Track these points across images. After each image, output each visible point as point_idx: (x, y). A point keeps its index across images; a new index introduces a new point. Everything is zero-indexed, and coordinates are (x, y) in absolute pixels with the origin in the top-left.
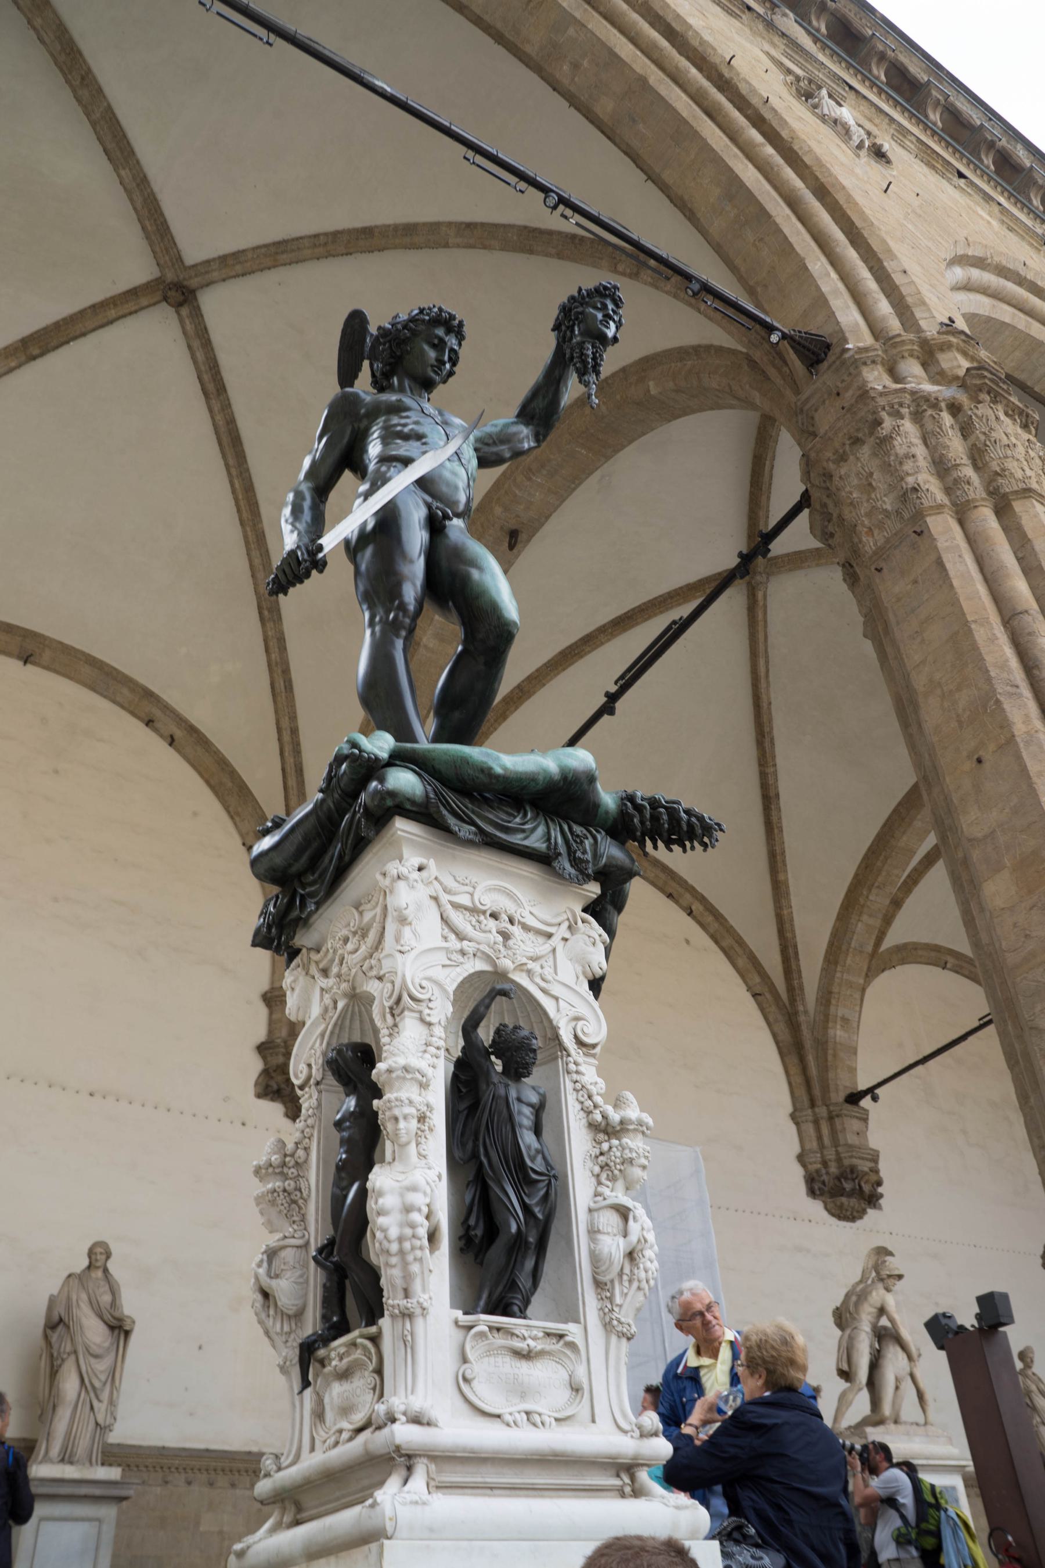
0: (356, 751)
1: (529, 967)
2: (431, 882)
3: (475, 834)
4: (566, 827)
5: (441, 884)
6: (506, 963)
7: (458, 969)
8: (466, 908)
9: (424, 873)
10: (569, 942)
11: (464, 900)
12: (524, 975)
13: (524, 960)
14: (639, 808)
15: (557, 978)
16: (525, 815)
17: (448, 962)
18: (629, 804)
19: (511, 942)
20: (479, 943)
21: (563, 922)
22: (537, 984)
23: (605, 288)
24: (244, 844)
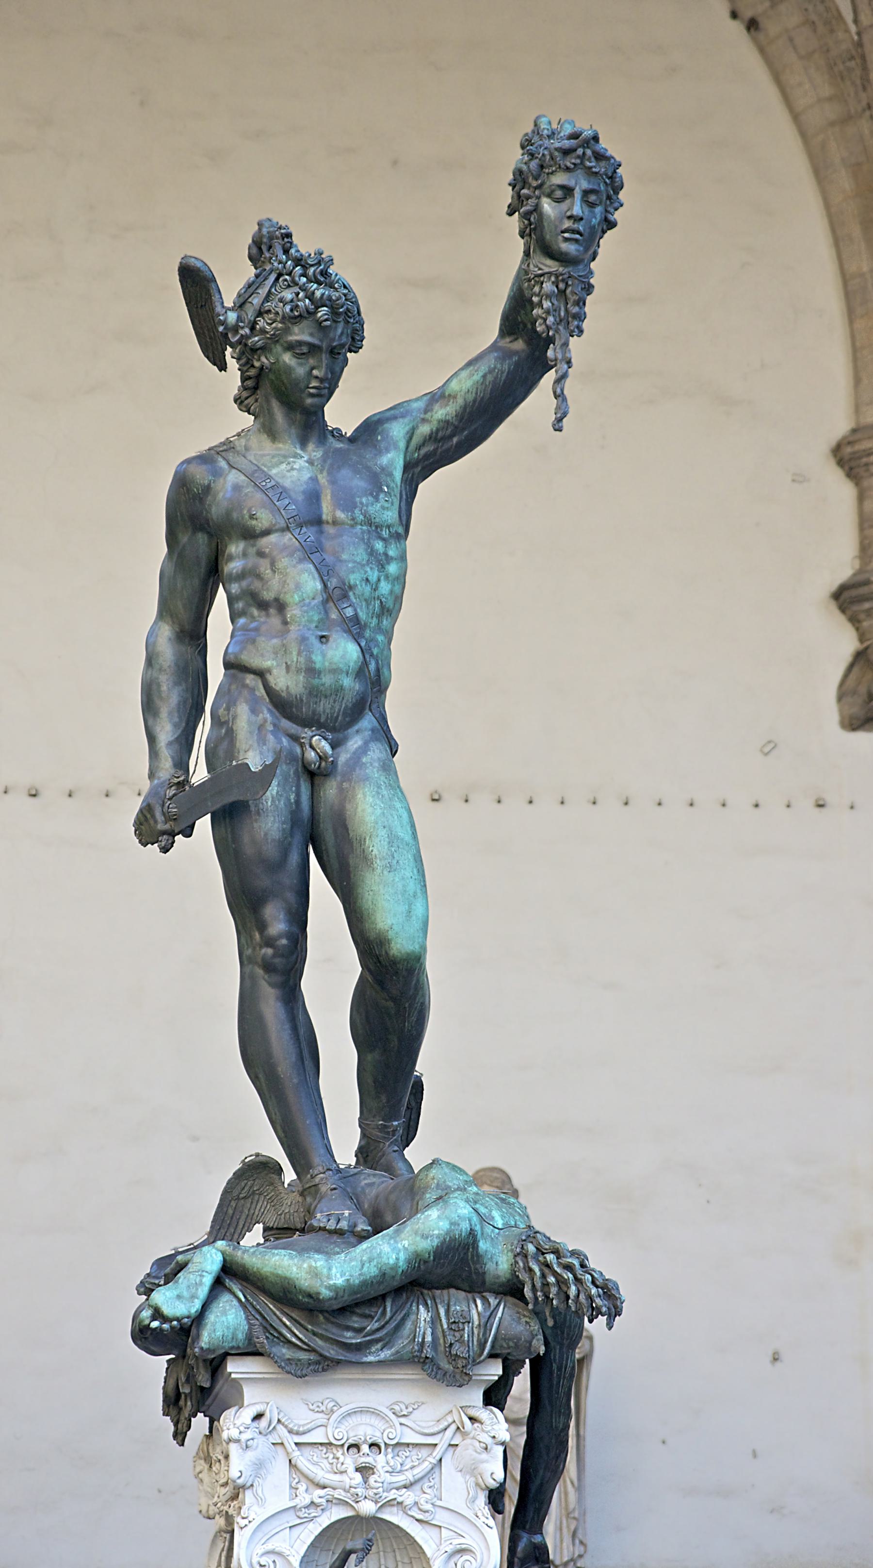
0: (155, 1324)
1: (400, 1499)
2: (274, 1428)
3: (318, 1363)
4: (442, 1312)
5: (286, 1427)
6: (367, 1508)
7: (311, 1525)
8: (321, 1444)
9: (264, 1423)
10: (459, 1448)
11: (317, 1436)
12: (395, 1509)
13: (393, 1494)
14: (531, 1270)
15: (438, 1503)
16: (384, 1313)
17: (299, 1521)
18: (521, 1264)
19: (372, 1479)
20: (334, 1489)
21: (449, 1426)
22: (412, 1516)
23: (566, 152)
24: (734, 15)
